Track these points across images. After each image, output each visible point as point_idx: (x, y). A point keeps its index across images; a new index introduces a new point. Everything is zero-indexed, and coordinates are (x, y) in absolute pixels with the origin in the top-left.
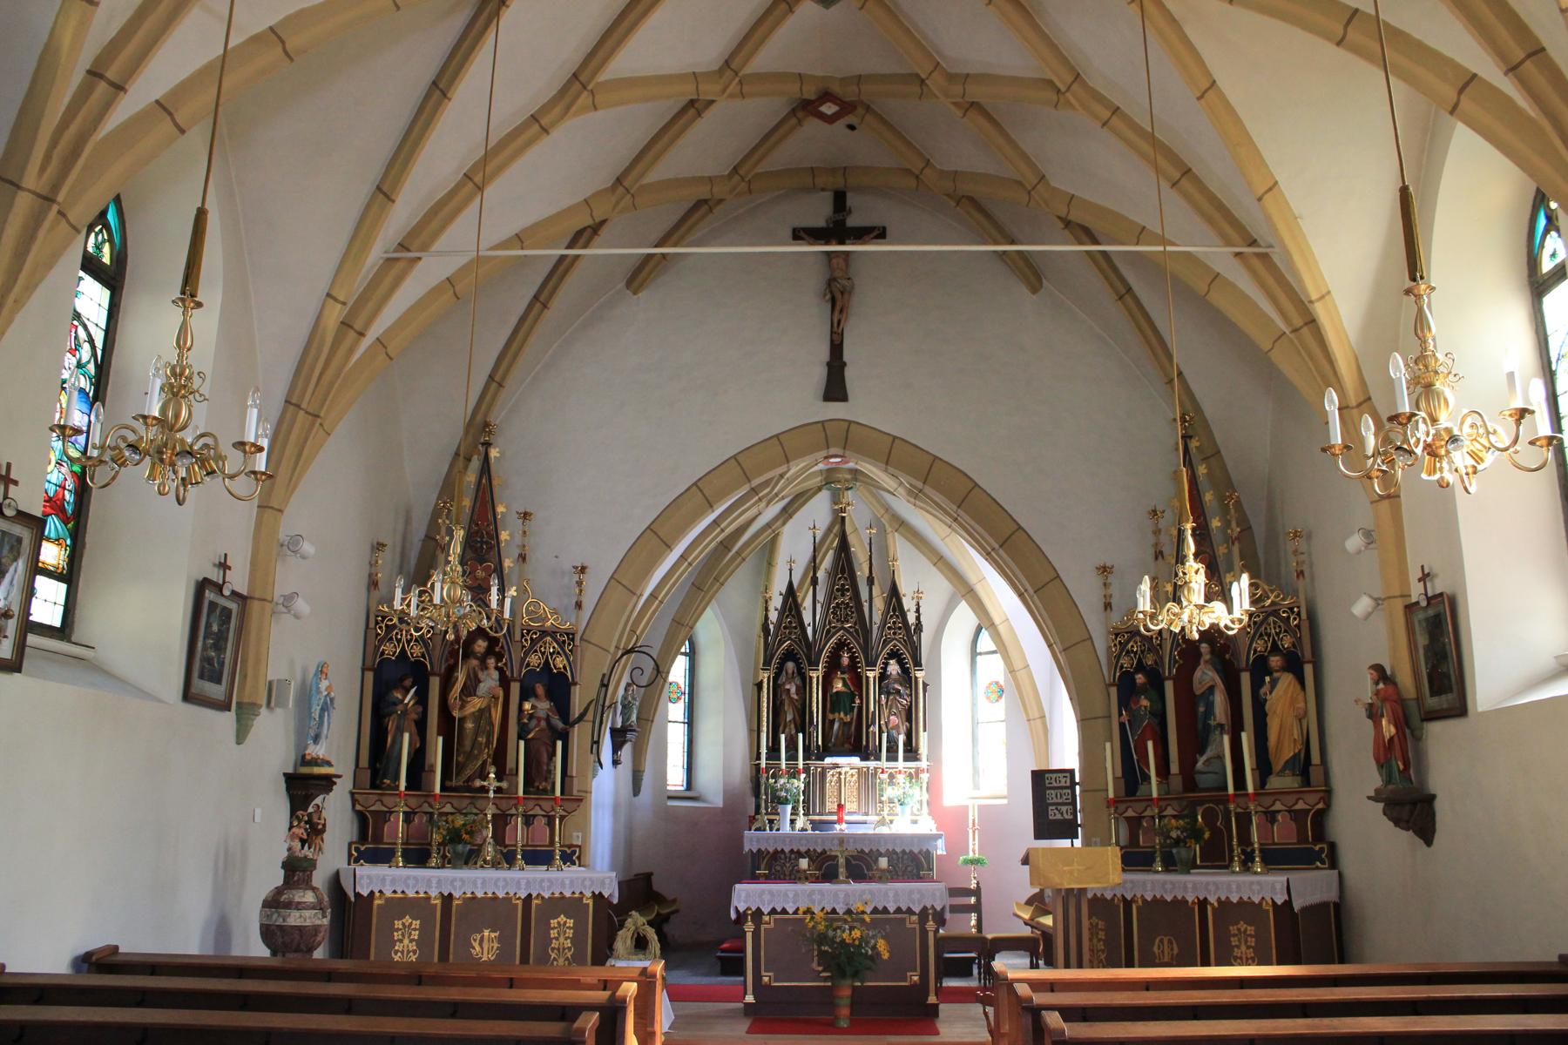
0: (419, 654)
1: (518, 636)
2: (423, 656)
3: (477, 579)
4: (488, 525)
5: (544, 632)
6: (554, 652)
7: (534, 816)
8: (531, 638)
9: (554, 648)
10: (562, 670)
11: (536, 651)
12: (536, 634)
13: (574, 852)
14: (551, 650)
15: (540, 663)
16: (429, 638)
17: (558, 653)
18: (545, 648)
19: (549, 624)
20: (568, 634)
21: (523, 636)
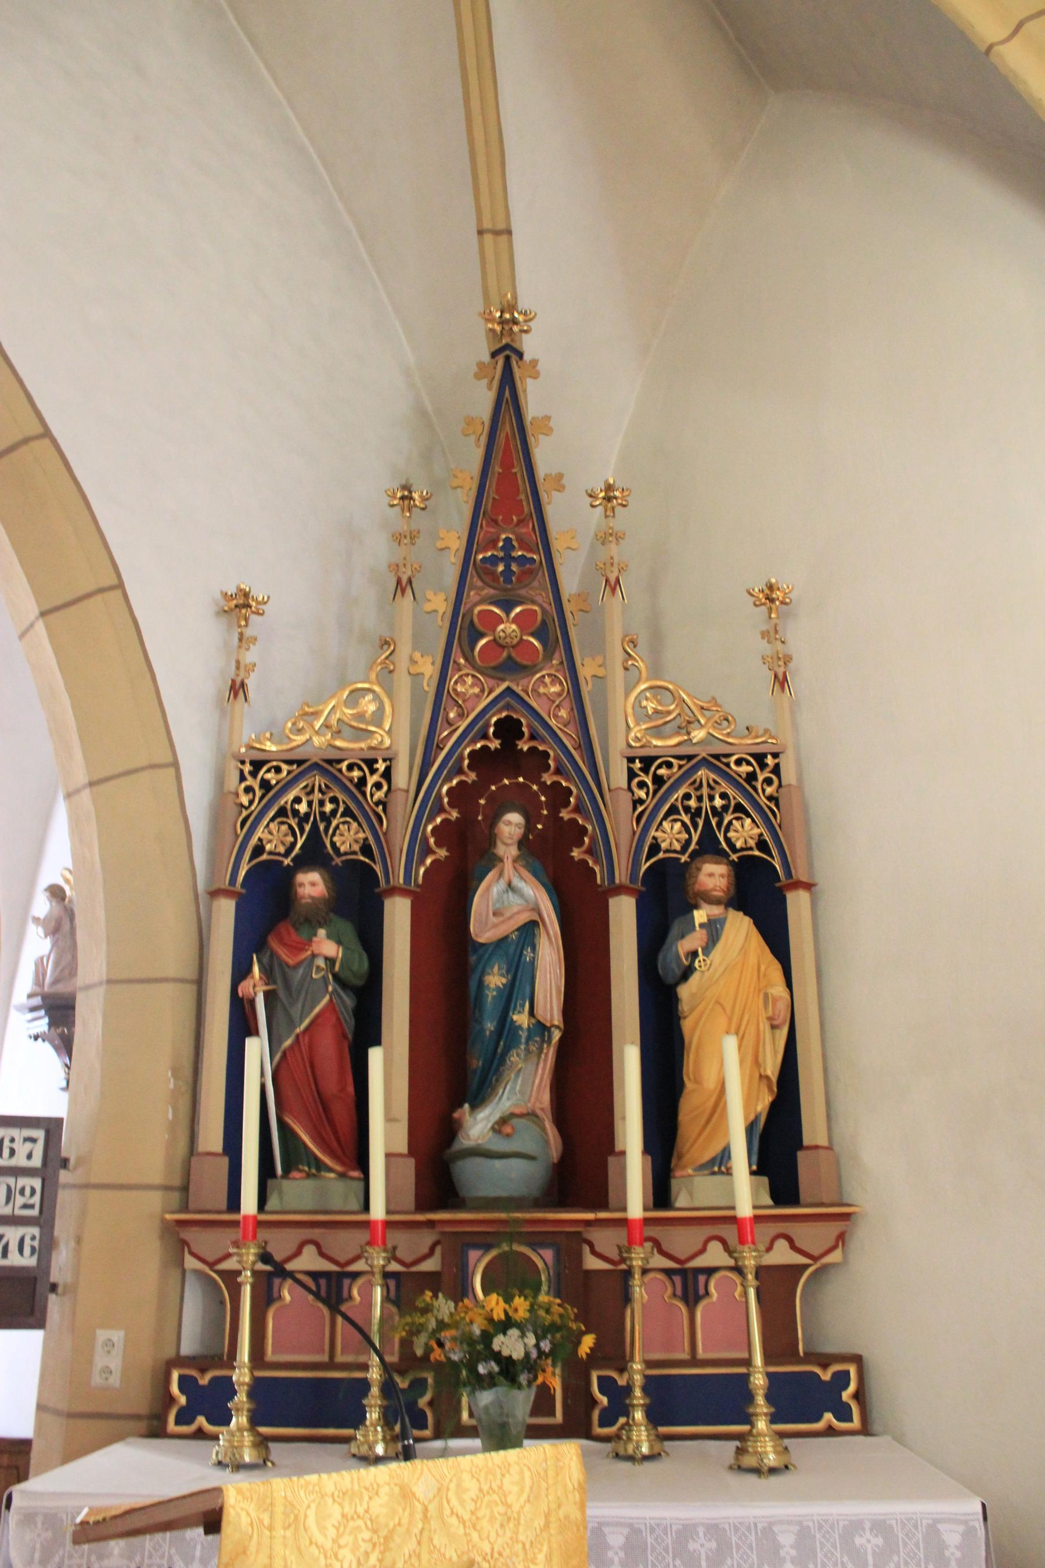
0: (356, 848)
1: (619, 778)
2: (366, 849)
3: (503, 647)
4: (520, 522)
5: (690, 758)
6: (725, 808)
7: (710, 1271)
8: (658, 781)
9: (724, 796)
10: (757, 853)
11: (673, 810)
12: (669, 765)
13: (842, 1379)
14: (718, 802)
15: (688, 842)
16: (377, 804)
17: (739, 808)
18: (700, 799)
19: (698, 735)
20: (760, 758)
21: (632, 774)
